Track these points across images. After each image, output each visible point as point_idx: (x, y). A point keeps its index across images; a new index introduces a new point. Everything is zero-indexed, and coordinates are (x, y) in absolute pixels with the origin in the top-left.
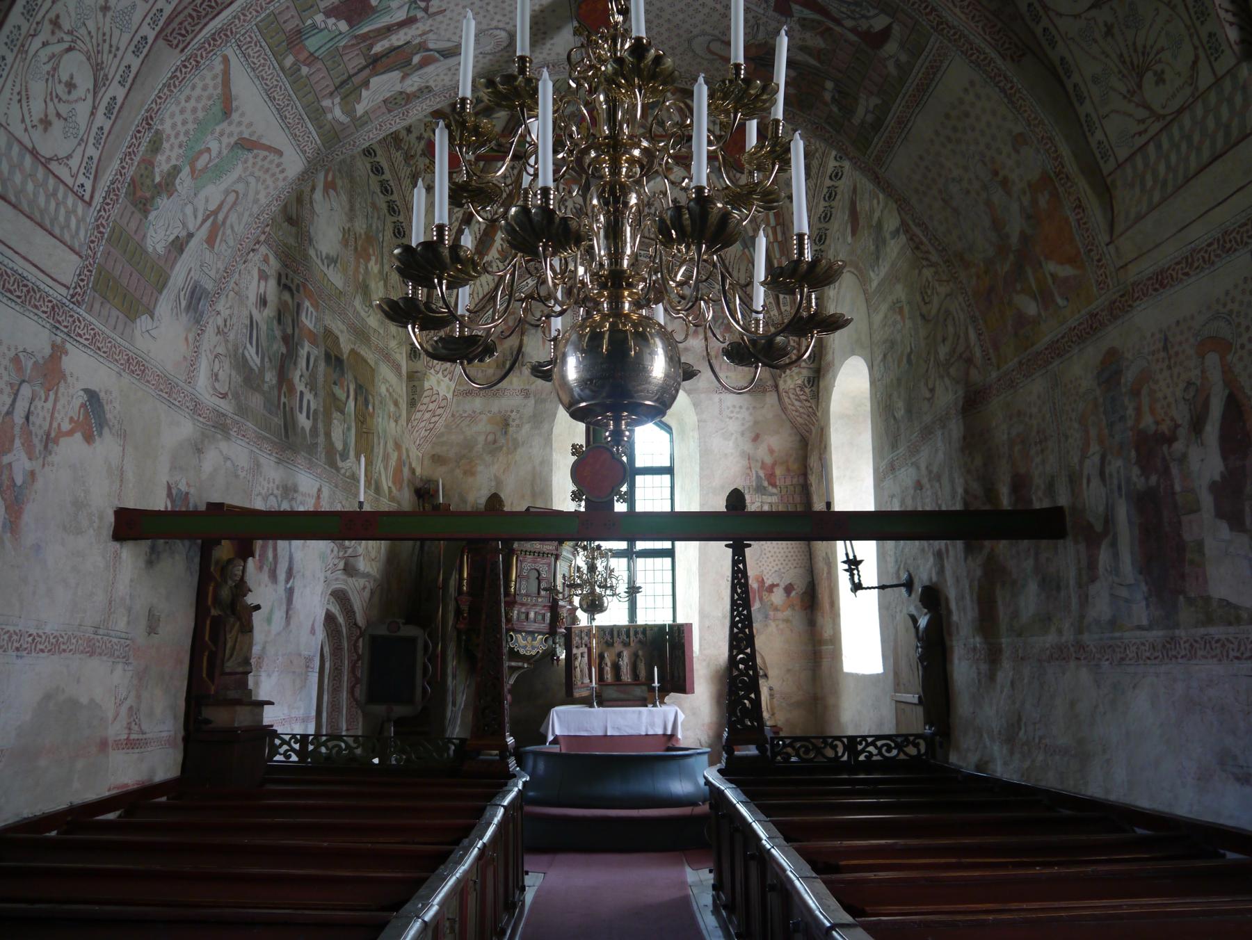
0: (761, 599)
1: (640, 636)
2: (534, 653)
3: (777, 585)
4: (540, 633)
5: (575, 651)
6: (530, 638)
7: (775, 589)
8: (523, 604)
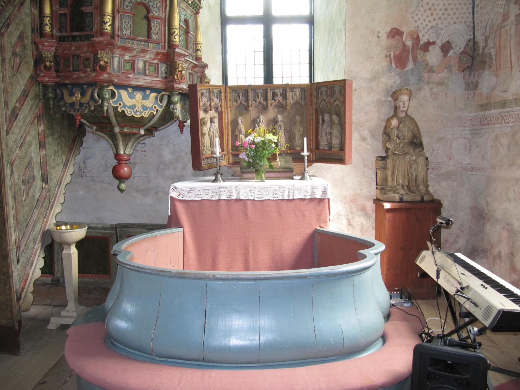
0: (415, 59)
1: (279, 98)
2: (146, 114)
3: (434, 43)
4: (153, 90)
5: (201, 115)
6: (139, 95)
7: (431, 48)
8: (126, 49)
